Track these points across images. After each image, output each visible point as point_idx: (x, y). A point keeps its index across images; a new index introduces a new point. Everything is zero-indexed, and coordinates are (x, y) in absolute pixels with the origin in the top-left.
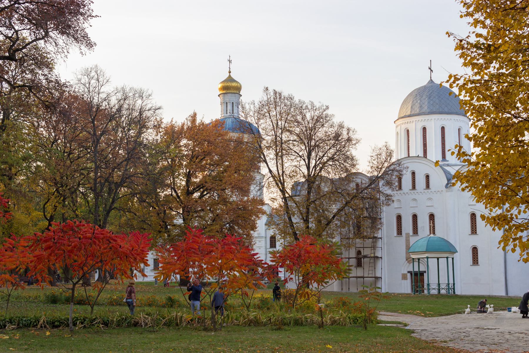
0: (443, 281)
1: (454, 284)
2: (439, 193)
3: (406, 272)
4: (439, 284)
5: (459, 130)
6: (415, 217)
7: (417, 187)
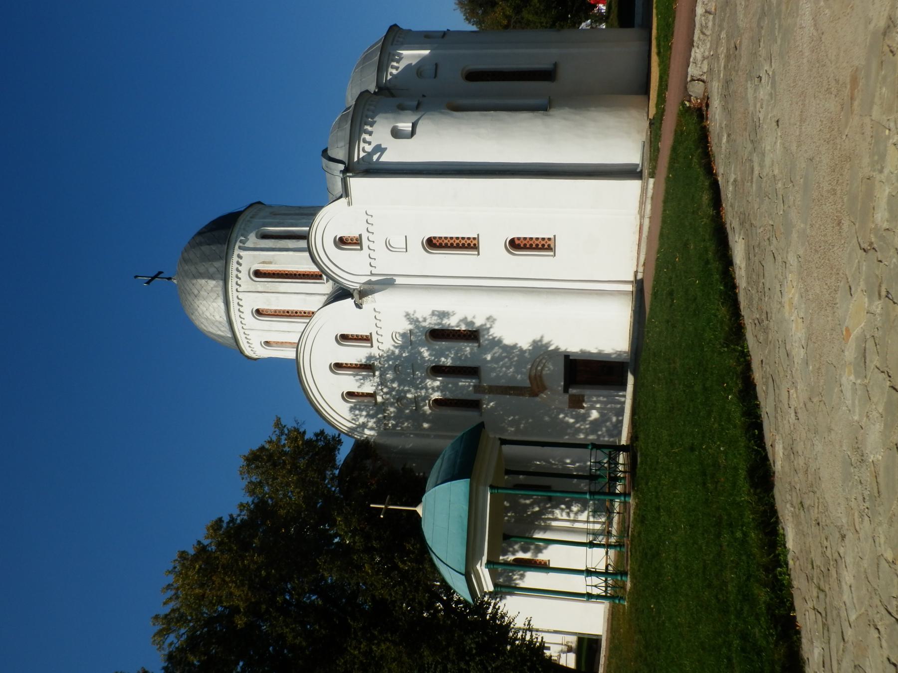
3: (566, 397)
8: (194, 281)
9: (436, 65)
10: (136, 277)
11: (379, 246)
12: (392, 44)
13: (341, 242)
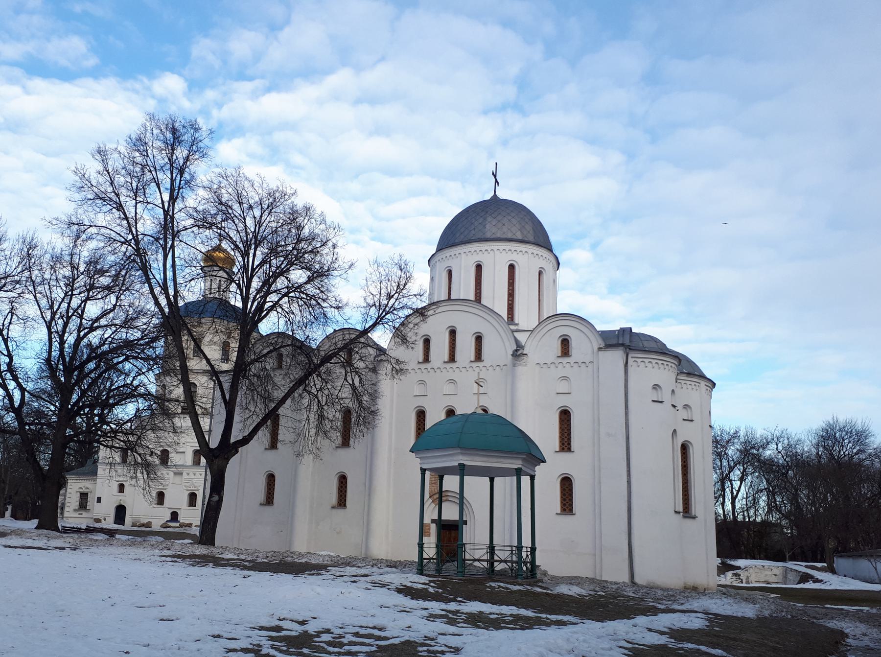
0: (504, 537)
1: (533, 549)
2: (498, 369)
5: (540, 273)
7: (458, 357)
9: (692, 421)
10: (496, 163)
12: (706, 385)
13: (565, 343)
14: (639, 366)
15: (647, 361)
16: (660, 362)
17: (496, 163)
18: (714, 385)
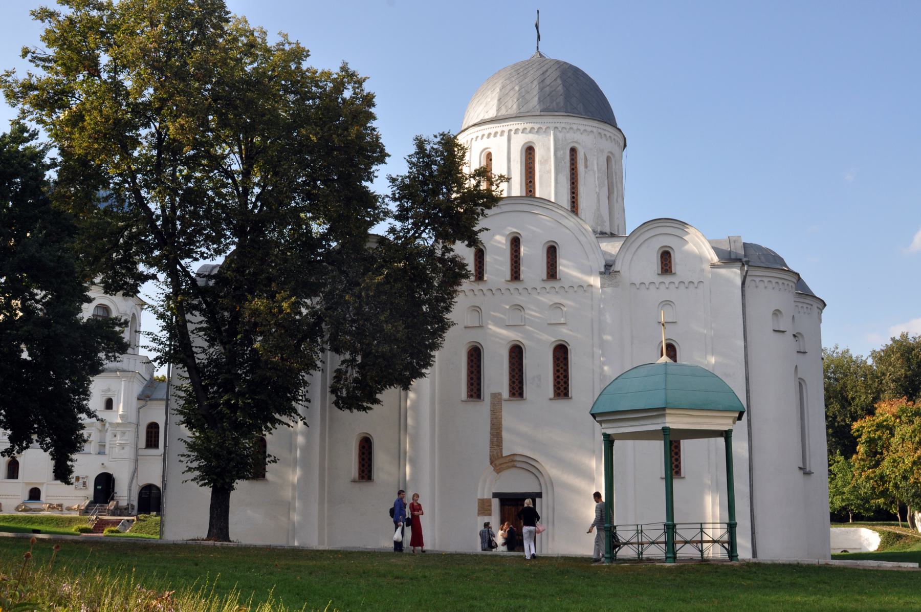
3: (488, 495)
4: (670, 528)
6: (516, 353)
8: (559, 81)
10: (538, 11)
11: (664, 294)
12: (818, 307)
14: (757, 287)
15: (766, 280)
16: (780, 282)
17: (538, 11)
18: (825, 305)
